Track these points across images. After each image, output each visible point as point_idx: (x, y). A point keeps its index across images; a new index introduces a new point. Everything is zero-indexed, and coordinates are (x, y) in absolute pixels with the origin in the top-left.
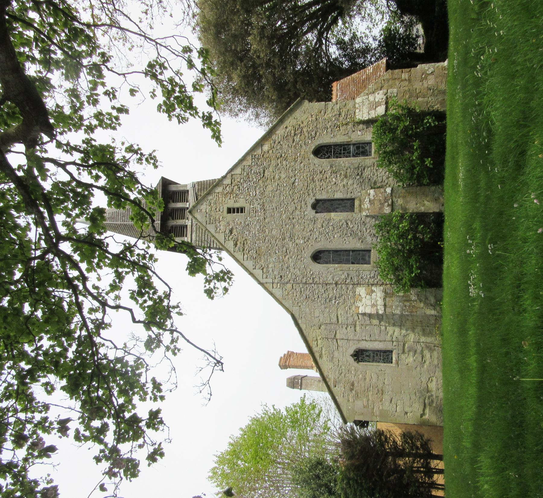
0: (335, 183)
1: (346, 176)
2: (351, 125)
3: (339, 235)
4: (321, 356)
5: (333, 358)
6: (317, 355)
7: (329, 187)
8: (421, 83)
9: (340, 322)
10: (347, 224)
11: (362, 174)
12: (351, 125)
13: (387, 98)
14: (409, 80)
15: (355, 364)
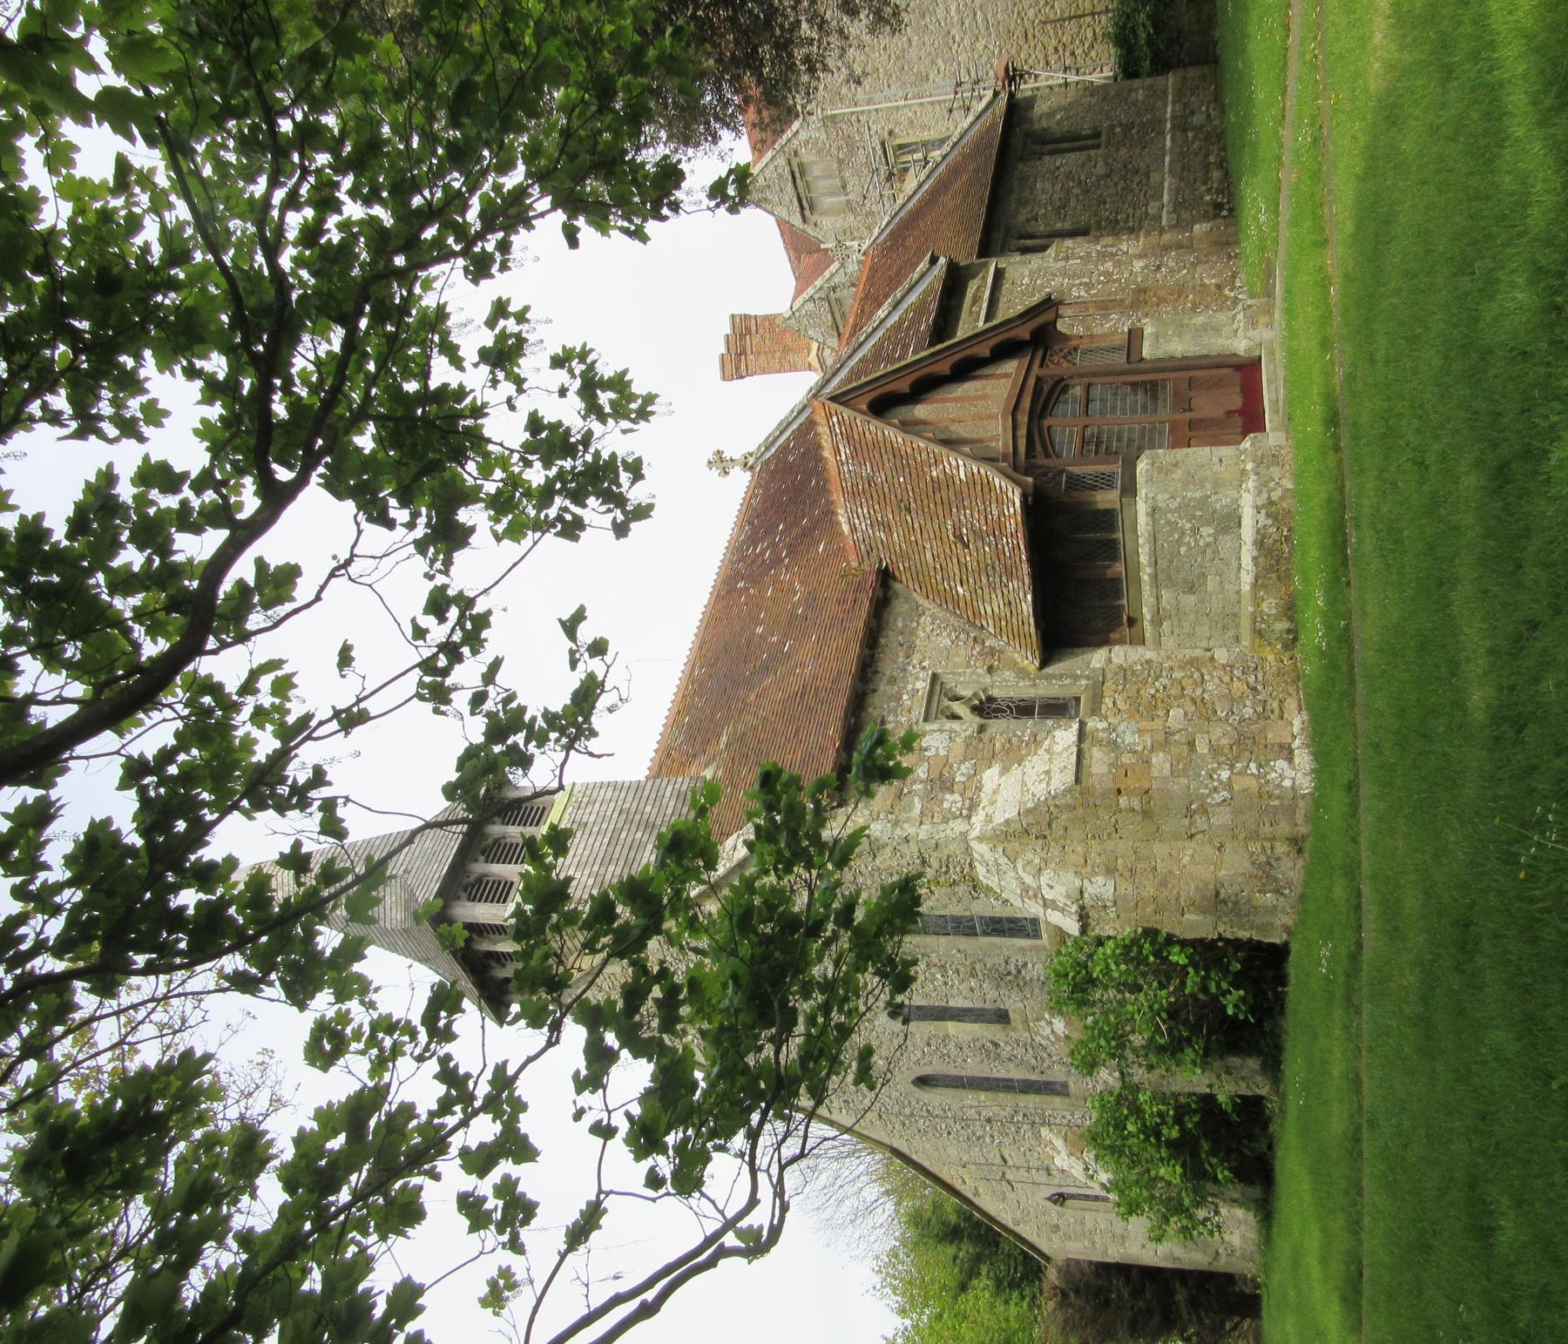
0: (946, 983)
1: (973, 974)
2: (962, 889)
3: (978, 1059)
4: (976, 1194)
5: (1004, 1199)
6: (969, 1195)
7: (927, 990)
8: (1186, 822)
9: (1010, 1163)
10: (996, 1045)
11: (1019, 972)
12: (962, 889)
13: (1082, 908)
14: (1146, 813)
15: (1058, 1208)
